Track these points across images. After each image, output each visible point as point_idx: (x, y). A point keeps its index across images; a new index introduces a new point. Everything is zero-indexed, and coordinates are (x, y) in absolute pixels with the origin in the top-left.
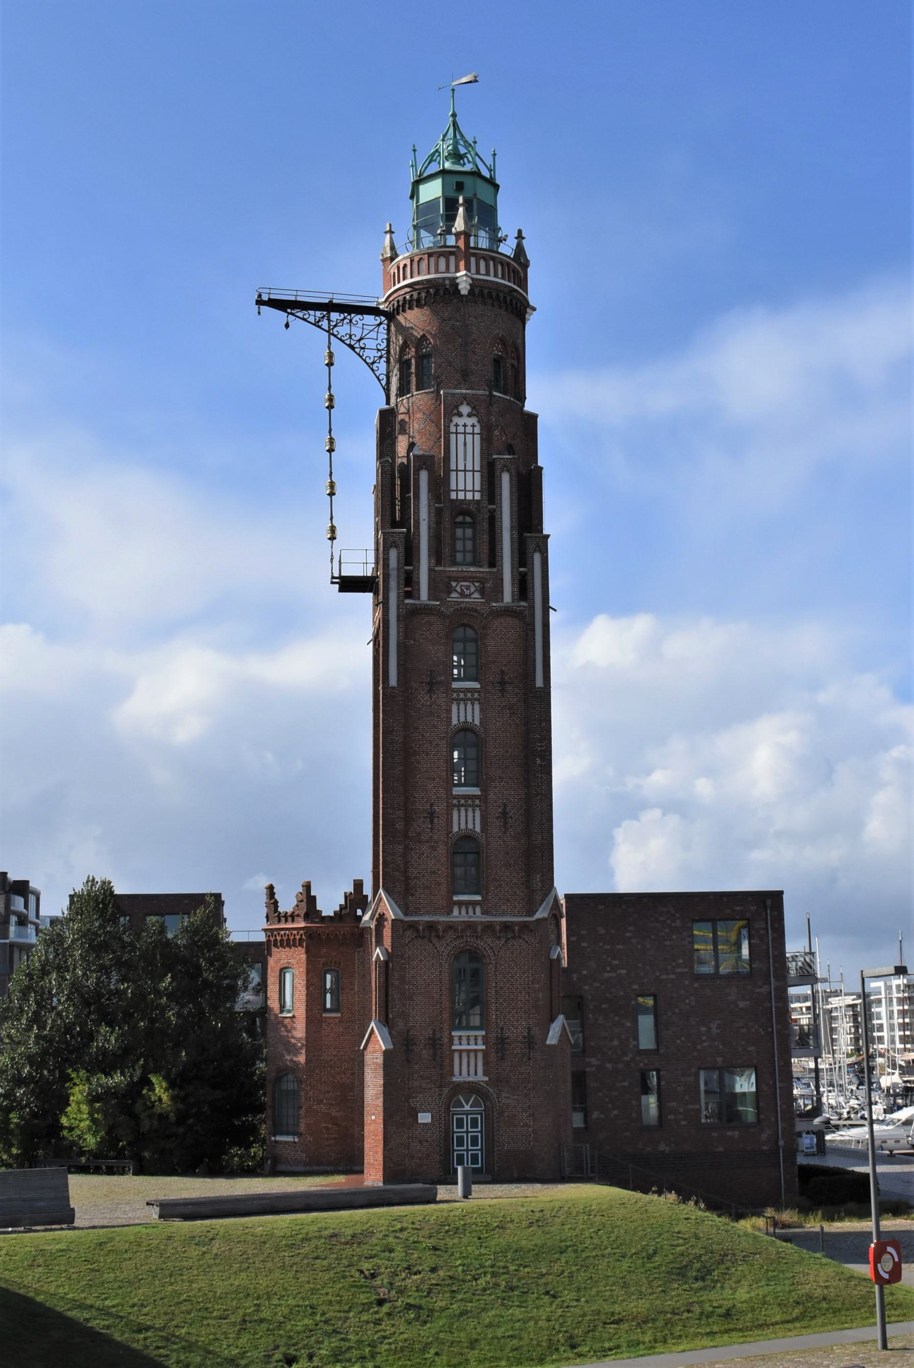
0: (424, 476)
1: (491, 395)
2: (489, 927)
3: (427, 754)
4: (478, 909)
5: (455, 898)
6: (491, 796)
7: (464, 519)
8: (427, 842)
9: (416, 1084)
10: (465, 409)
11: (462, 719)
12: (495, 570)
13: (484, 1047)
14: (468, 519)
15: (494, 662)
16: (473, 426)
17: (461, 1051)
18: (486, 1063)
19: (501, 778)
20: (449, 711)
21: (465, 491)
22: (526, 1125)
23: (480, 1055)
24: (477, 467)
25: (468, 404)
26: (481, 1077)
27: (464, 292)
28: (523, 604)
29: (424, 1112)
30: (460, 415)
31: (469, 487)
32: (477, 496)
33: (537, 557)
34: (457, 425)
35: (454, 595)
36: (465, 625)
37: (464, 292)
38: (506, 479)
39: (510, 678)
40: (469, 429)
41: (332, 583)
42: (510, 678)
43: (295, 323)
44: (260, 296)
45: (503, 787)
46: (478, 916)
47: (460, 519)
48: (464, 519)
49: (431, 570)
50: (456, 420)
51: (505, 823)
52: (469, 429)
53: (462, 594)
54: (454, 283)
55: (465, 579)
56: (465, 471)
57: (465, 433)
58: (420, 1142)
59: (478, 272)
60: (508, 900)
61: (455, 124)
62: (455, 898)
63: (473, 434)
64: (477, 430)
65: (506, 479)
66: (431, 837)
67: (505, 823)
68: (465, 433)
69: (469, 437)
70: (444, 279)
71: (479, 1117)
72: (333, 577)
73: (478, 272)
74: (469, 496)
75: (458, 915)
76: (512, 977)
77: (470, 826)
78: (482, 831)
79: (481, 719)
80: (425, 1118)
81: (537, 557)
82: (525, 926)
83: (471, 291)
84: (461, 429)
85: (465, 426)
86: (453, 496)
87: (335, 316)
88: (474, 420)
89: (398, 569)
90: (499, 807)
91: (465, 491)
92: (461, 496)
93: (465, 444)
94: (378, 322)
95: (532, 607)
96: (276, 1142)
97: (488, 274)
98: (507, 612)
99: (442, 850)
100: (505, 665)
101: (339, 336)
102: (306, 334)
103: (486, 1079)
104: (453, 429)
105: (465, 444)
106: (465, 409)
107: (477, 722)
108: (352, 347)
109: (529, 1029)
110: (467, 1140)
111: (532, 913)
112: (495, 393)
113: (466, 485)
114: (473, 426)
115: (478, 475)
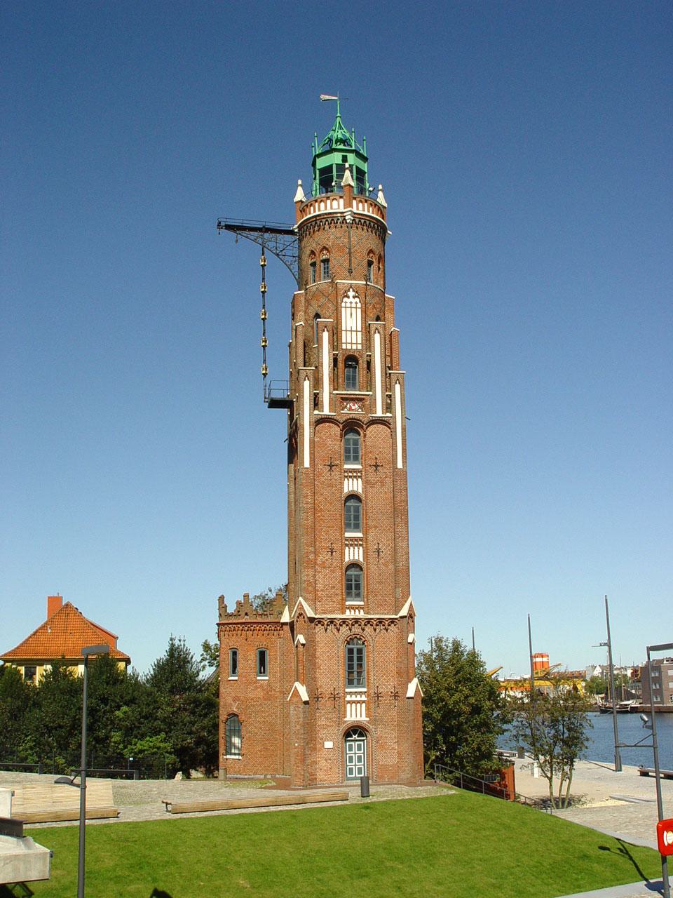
0: (326, 335)
1: (366, 284)
2: (369, 621)
4: (362, 611)
5: (347, 603)
6: (370, 538)
8: (329, 567)
9: (324, 723)
10: (351, 293)
12: (371, 393)
13: (366, 699)
15: (371, 452)
16: (356, 303)
17: (351, 702)
18: (368, 709)
20: (342, 484)
21: (352, 343)
22: (393, 748)
23: (364, 705)
24: (359, 329)
25: (353, 290)
26: (364, 718)
28: (389, 415)
29: (328, 740)
30: (348, 297)
31: (354, 341)
32: (360, 347)
34: (346, 303)
35: (346, 410)
38: (377, 337)
40: (354, 305)
41: (265, 402)
43: (242, 240)
44: (220, 223)
46: (361, 614)
49: (330, 393)
50: (345, 299)
51: (379, 555)
53: (350, 409)
55: (352, 400)
57: (351, 307)
58: (326, 760)
59: (358, 209)
60: (381, 605)
62: (347, 603)
63: (356, 308)
64: (359, 305)
65: (377, 337)
67: (379, 555)
68: (351, 307)
69: (354, 310)
70: (337, 213)
71: (362, 743)
72: (265, 398)
73: (358, 209)
74: (354, 347)
75: (349, 614)
76: (384, 654)
78: (364, 559)
80: (329, 744)
82: (393, 621)
84: (348, 305)
85: (351, 303)
87: (267, 235)
88: (357, 300)
91: (352, 343)
92: (349, 347)
94: (294, 239)
95: (394, 417)
96: (227, 759)
97: (364, 210)
100: (378, 454)
101: (269, 248)
102: (248, 245)
103: (368, 719)
104: (343, 305)
106: (351, 293)
107: (360, 490)
108: (278, 255)
109: (395, 687)
110: (355, 758)
111: (396, 612)
112: (368, 283)
114: (356, 303)
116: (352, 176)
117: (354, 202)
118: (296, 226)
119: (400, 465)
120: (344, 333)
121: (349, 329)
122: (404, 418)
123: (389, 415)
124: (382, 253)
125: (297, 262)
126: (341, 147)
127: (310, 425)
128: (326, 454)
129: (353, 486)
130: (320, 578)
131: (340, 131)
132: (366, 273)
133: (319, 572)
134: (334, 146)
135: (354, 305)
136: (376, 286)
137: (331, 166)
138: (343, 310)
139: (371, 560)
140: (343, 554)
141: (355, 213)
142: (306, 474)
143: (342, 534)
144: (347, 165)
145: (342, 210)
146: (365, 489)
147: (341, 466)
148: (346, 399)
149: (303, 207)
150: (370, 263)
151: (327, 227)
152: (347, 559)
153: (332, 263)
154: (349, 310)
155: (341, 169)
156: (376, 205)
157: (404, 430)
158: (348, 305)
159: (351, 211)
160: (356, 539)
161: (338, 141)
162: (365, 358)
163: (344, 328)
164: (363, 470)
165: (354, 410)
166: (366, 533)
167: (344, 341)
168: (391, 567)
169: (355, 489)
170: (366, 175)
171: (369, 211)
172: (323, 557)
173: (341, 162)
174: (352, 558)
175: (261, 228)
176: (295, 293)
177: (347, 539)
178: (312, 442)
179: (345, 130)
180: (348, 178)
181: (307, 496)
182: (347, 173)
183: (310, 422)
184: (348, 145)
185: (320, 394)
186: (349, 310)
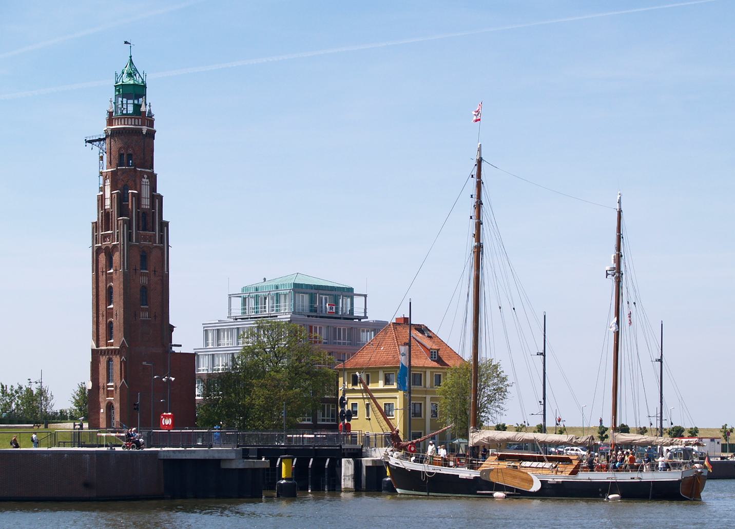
10: (146, 176)
24: (149, 197)
27: (144, 133)
28: (162, 245)
30: (144, 178)
32: (149, 207)
33: (165, 228)
37: (144, 133)
50: (143, 179)
54: (141, 130)
61: (131, 60)
64: (149, 184)
81: (165, 228)
83: (146, 133)
84: (144, 183)
88: (148, 180)
91: (145, 205)
98: (156, 247)
113: (146, 203)
129: (144, 280)
135: (146, 184)
158: (144, 183)
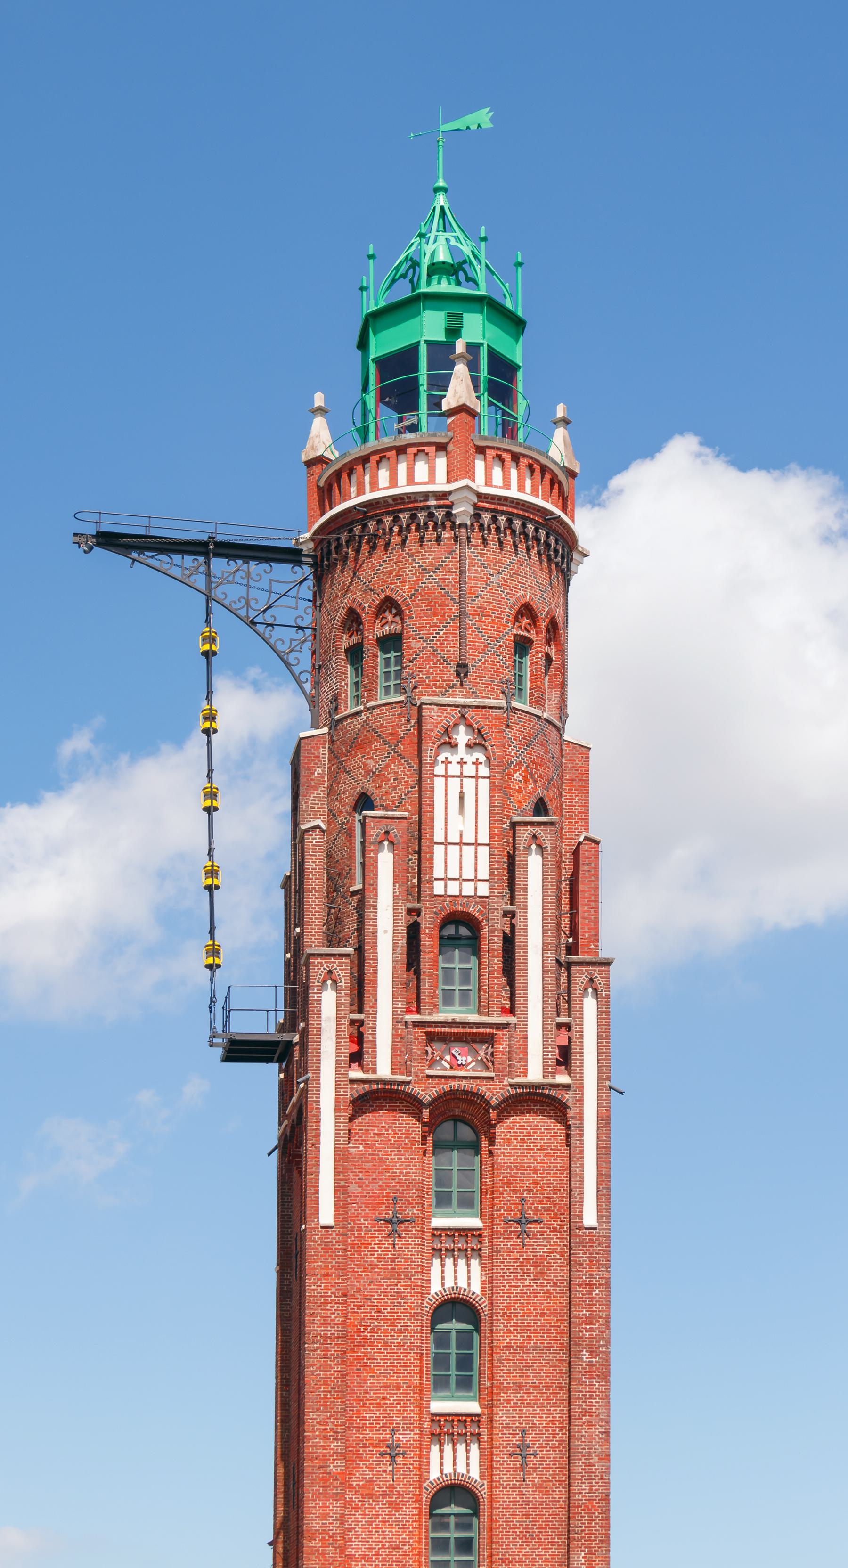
3: (386, 1344)
7: (457, 930)
8: (384, 1495)
11: (449, 1283)
12: (511, 1019)
14: (464, 931)
16: (477, 763)
19: (520, 1386)
20: (425, 1270)
24: (484, 838)
28: (562, 1079)
30: (453, 746)
31: (468, 873)
34: (447, 762)
36: (456, 1120)
39: (536, 1211)
40: (469, 770)
42: (536, 1211)
45: (522, 1400)
47: (450, 930)
48: (457, 930)
49: (396, 1021)
52: (469, 770)
56: (461, 844)
57: (461, 776)
59: (488, 482)
63: (476, 777)
64: (484, 771)
66: (392, 1487)
68: (461, 776)
70: (426, 495)
73: (488, 482)
74: (468, 889)
77: (461, 1469)
78: (482, 1476)
79: (483, 1282)
84: (454, 769)
85: (462, 763)
86: (438, 888)
89: (338, 1019)
90: (514, 1435)
92: (453, 889)
93: (462, 798)
97: (507, 485)
99: (410, 1509)
104: (439, 769)
105: (462, 798)
106: (462, 737)
107: (476, 1288)
113: (461, 869)
114: (477, 763)
115: (484, 852)
116: (475, 381)
117: (480, 465)
118: (308, 535)
119: (590, 1218)
120: (438, 850)
121: (453, 837)
122: (605, 1089)
123: (562, 1079)
124: (559, 612)
125: (308, 644)
126: (444, 286)
127: (337, 1109)
128: (381, 1188)
130: (358, 1522)
131: (442, 236)
132: (508, 674)
133: (357, 1508)
134: (424, 289)
136: (538, 712)
137: (413, 350)
138: (439, 783)
139: (502, 1475)
140: (423, 1463)
141: (480, 496)
142: (327, 1246)
143: (422, 1407)
144: (460, 347)
145: (441, 485)
146: (489, 1284)
147: (423, 1220)
148: (440, 1036)
149: (330, 481)
150: (522, 646)
151: (396, 539)
152: (434, 1474)
153: (413, 644)
154: (454, 784)
155: (442, 355)
156: (544, 469)
157: (604, 1121)
158: (454, 769)
159: (467, 487)
160: (463, 1418)
161: (436, 269)
162: (501, 925)
163: (439, 836)
164: (485, 1233)
165: (463, 1066)
166: (489, 1401)
167: (438, 872)
168: (558, 1492)
169: (462, 1283)
170: (520, 375)
171: (521, 488)
172: (370, 1468)
173: (441, 337)
174: (448, 1469)
175: (205, 544)
176: (303, 734)
177: (436, 1418)
178: (340, 1154)
179: (458, 233)
180: (459, 389)
181: (326, 1303)
182: (461, 370)
183: (337, 1102)
184: (469, 279)
185: (368, 1024)
186: (454, 784)
